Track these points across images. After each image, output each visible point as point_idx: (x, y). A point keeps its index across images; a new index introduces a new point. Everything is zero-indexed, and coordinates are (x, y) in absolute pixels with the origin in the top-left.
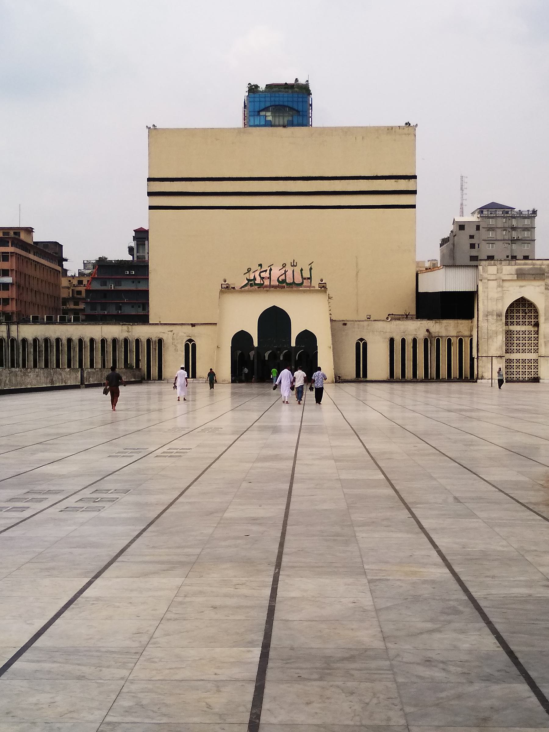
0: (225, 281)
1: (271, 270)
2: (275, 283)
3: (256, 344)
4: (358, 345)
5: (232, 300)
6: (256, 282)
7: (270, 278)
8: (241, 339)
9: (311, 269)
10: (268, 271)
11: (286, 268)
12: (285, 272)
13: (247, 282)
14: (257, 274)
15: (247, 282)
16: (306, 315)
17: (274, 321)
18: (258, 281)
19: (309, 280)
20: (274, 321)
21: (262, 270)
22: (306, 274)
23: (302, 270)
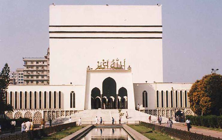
0: (89, 67)
1: (108, 62)
2: (109, 67)
3: (101, 93)
4: (143, 93)
5: (92, 75)
6: (102, 67)
7: (107, 66)
8: (95, 91)
9: (125, 62)
10: (107, 63)
11: (115, 61)
12: (114, 63)
13: (98, 67)
14: (102, 63)
15: (98, 67)
16: (122, 81)
17: (109, 83)
18: (103, 66)
19: (124, 67)
20: (109, 83)
21: (104, 62)
22: (123, 64)
23: (121, 62)
